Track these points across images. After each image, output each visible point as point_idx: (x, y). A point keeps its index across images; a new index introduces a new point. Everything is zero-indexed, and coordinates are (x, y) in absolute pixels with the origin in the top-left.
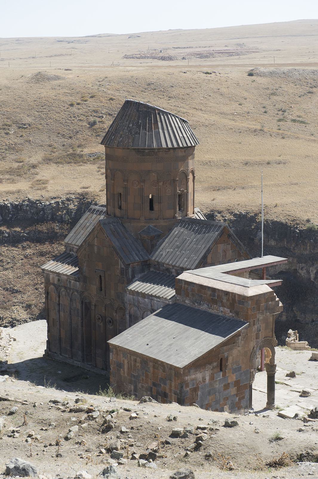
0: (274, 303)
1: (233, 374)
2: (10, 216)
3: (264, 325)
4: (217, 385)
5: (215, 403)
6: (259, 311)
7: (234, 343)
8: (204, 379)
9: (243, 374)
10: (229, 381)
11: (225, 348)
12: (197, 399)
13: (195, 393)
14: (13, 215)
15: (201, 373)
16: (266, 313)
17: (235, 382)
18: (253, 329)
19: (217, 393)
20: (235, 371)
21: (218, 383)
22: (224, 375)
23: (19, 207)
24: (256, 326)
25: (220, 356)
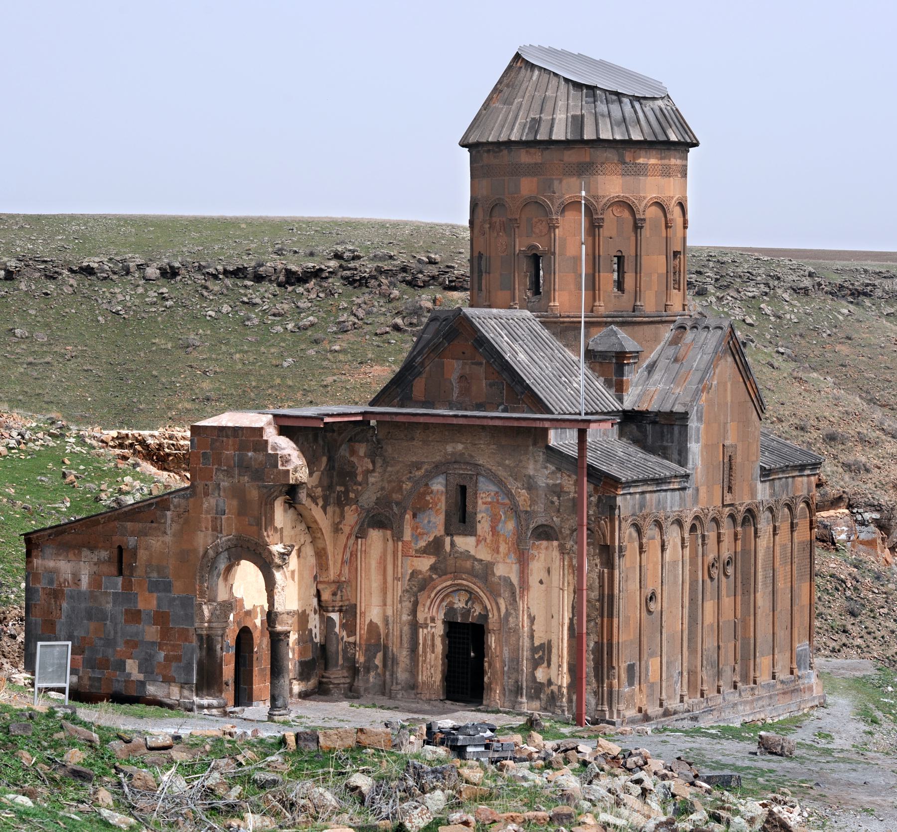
0: (261, 457)
1: (151, 591)
3: (235, 503)
4: (108, 603)
5: (102, 642)
6: (220, 465)
7: (152, 522)
8: (77, 580)
9: (177, 602)
10: (141, 606)
11: (129, 525)
12: (60, 618)
13: (55, 602)
15: (69, 561)
16: (240, 475)
17: (156, 612)
18: (202, 503)
19: (108, 622)
20: (154, 587)
21: (110, 599)
22: (128, 585)
24: (212, 501)
25: (117, 540)
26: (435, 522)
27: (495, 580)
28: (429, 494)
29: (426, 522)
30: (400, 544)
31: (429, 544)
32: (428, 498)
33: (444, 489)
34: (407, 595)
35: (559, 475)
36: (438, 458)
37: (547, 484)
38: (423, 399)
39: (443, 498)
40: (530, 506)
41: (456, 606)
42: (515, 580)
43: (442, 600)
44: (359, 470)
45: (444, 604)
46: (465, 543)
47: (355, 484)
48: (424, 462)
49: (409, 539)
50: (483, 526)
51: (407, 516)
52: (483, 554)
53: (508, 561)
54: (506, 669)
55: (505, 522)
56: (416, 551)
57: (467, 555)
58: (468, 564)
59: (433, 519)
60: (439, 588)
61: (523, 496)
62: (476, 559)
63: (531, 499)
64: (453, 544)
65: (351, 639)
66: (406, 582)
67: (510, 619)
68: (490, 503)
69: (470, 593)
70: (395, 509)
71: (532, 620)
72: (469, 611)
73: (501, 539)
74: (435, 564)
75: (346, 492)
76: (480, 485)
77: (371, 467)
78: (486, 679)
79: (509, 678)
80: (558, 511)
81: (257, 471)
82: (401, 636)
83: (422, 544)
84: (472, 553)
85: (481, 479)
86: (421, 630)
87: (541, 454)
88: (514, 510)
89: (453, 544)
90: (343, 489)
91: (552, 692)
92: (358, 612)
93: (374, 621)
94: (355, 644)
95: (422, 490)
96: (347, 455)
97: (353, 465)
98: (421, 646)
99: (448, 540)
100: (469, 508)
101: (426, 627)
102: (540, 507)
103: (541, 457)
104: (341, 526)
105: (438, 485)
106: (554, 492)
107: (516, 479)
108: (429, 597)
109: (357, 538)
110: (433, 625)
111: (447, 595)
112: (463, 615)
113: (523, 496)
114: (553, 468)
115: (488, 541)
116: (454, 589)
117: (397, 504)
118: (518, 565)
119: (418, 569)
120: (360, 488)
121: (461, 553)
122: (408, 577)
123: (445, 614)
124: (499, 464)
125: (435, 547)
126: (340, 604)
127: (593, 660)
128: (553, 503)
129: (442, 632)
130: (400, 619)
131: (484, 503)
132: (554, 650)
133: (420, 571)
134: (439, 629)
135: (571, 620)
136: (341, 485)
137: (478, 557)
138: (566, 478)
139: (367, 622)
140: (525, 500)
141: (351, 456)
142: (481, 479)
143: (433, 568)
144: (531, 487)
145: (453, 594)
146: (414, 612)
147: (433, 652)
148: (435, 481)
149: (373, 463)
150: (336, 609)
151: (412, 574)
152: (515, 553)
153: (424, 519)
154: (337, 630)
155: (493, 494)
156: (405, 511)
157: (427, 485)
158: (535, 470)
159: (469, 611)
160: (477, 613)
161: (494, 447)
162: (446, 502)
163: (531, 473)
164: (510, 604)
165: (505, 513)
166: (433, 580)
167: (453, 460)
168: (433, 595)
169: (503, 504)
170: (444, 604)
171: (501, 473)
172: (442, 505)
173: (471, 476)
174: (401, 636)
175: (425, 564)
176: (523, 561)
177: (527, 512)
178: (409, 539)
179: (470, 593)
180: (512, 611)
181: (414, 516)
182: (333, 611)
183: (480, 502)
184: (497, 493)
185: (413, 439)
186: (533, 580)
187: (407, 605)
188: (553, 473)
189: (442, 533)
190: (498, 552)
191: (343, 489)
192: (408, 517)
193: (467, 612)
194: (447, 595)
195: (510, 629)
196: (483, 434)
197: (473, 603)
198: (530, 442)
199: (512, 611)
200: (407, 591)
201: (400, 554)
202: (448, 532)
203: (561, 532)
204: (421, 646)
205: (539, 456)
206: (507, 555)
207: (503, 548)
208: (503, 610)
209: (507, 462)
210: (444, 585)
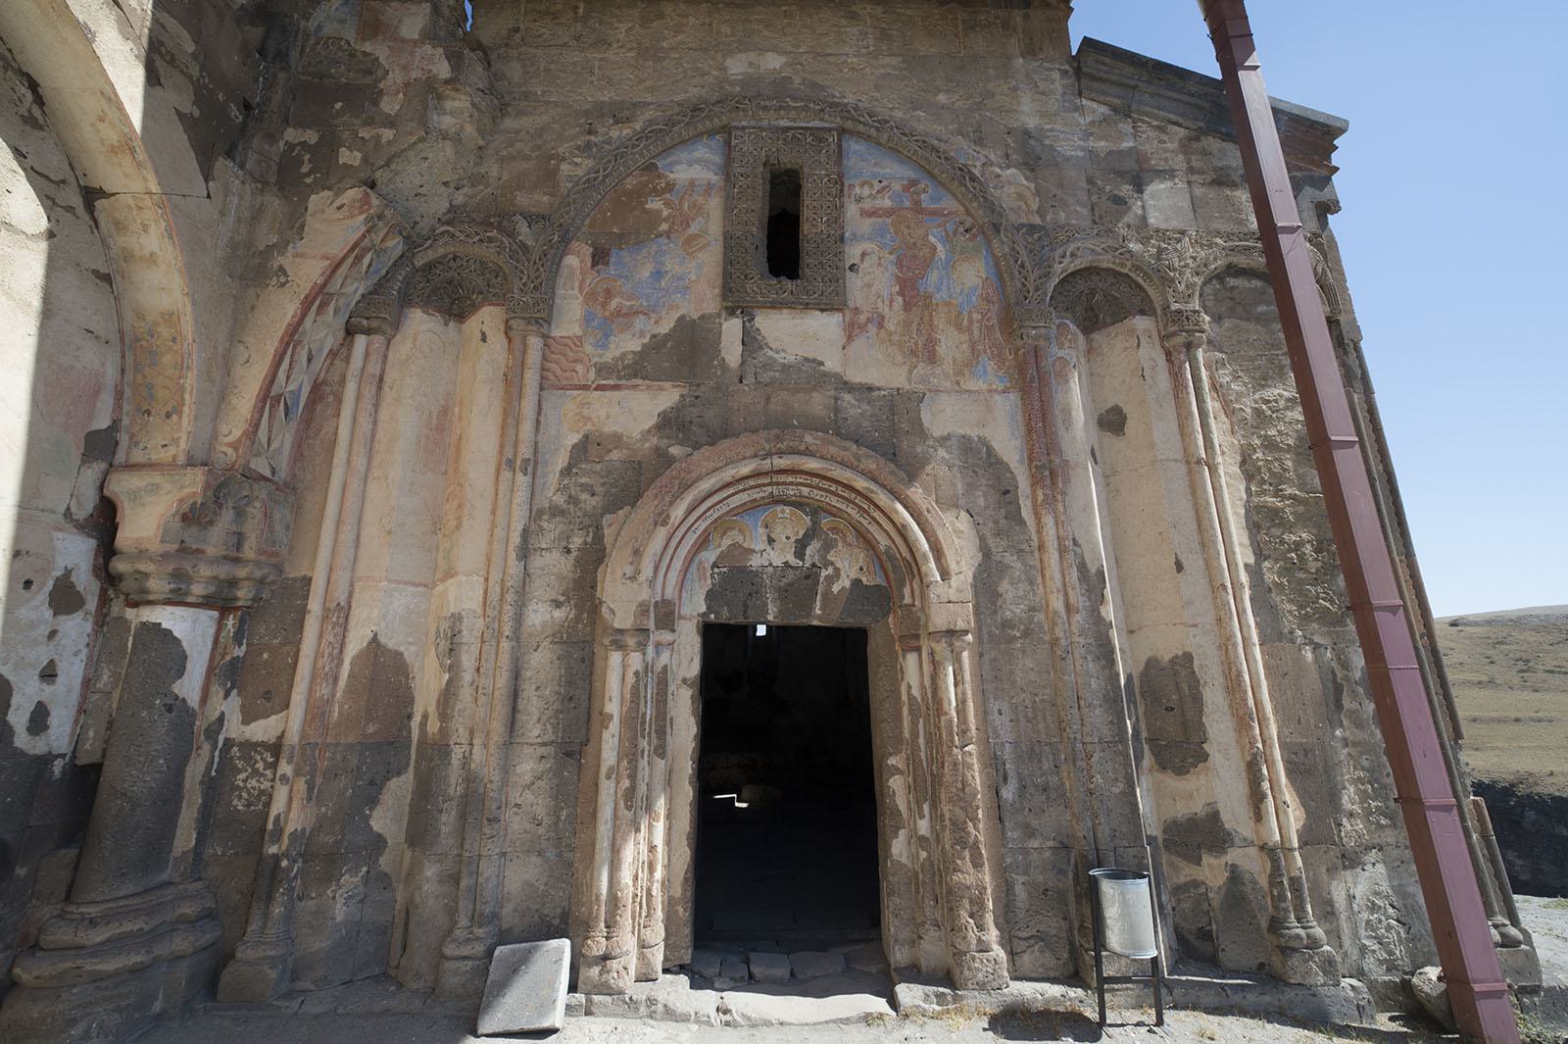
26: (686, 271)
28: (657, 192)
29: (646, 273)
30: (535, 343)
31: (657, 344)
32: (654, 204)
33: (715, 179)
34: (552, 528)
35: (1126, 127)
37: (1092, 153)
39: (715, 205)
40: (1041, 212)
41: (755, 562)
42: (1009, 447)
43: (703, 543)
44: (396, 77)
45: (710, 556)
46: (796, 333)
47: (369, 122)
48: (645, 104)
49: (576, 330)
50: (871, 279)
51: (571, 261)
52: (877, 367)
53: (972, 384)
54: (1008, 793)
55: (950, 265)
56: (601, 369)
57: (812, 376)
58: (817, 403)
59: (672, 265)
60: (706, 485)
61: (1012, 187)
62: (848, 386)
63: (1038, 193)
64: (751, 341)
65: (262, 730)
66: (553, 478)
67: (1004, 586)
68: (889, 213)
69: (815, 511)
70: (524, 231)
71: (1093, 584)
72: (811, 575)
73: (940, 322)
74: (677, 409)
75: (329, 145)
76: (851, 162)
77: (443, 70)
78: (899, 849)
79: (1030, 832)
82: (515, 694)
83: (628, 344)
84: (832, 365)
85: (854, 146)
86: (615, 658)
87: (1056, 75)
88: (987, 224)
89: (751, 341)
90: (311, 136)
91: (1235, 875)
92: (315, 605)
93: (389, 641)
94: (276, 748)
95: (630, 183)
96: (350, 34)
97: (371, 67)
98: (614, 727)
99: (732, 328)
100: (812, 225)
101: (642, 646)
102: (1075, 213)
103: (1057, 83)
104: (285, 260)
105: (694, 168)
107: (980, 142)
108: (662, 519)
109: (350, 332)
110: (666, 636)
111: (721, 526)
112: (784, 593)
113: (1012, 187)
114: (1104, 109)
115: (890, 326)
116: (756, 494)
117: (531, 219)
118: (1014, 397)
119: (609, 428)
120: (388, 134)
121: (786, 368)
122: (561, 460)
123: (710, 596)
124: (915, 106)
125: (685, 352)
126: (223, 571)
129: (694, 669)
130: (519, 619)
131: (865, 213)
132: (1214, 697)
133: (617, 440)
134: (684, 656)
135: (1255, 572)
136: (302, 124)
137: (856, 376)
138: (1152, 134)
139: (355, 644)
140: (1020, 197)
141: (364, 40)
142: (854, 146)
143: (671, 423)
144: (1032, 156)
145: (747, 520)
146: (584, 591)
147: (661, 751)
148: (682, 155)
149: (455, 59)
150: (198, 590)
151: (581, 450)
152: (999, 357)
153: (637, 268)
154: (189, 687)
155: (897, 186)
156: (565, 241)
157: (650, 168)
158: (1043, 115)
159: (811, 575)
160: (845, 582)
161: (895, 61)
162: (728, 209)
163: (1032, 123)
164: (998, 534)
165: (947, 239)
166: (668, 461)
168: (678, 511)
169: (934, 213)
170: (710, 556)
171: (922, 122)
172: (712, 223)
173: (819, 135)
174: (515, 694)
175: (635, 413)
176: (1034, 387)
177: (1032, 228)
178: (576, 330)
179: (815, 511)
180: (1010, 559)
181: (600, 257)
182: (177, 599)
183: (852, 210)
184: (913, 183)
185: (603, 42)
187: (553, 565)
188: (1105, 120)
189: (711, 304)
190: (932, 359)
191: (311, 136)
192: (574, 261)
193: (802, 584)
194: (721, 526)
195: (1006, 624)
196: (855, 31)
197: (828, 546)
198: (1014, 46)
199: (1010, 559)
200: (556, 512)
201: (531, 378)
202: (736, 304)
204: (614, 727)
205: (1053, 81)
207: (950, 344)
209: (942, 98)
210: (728, 474)
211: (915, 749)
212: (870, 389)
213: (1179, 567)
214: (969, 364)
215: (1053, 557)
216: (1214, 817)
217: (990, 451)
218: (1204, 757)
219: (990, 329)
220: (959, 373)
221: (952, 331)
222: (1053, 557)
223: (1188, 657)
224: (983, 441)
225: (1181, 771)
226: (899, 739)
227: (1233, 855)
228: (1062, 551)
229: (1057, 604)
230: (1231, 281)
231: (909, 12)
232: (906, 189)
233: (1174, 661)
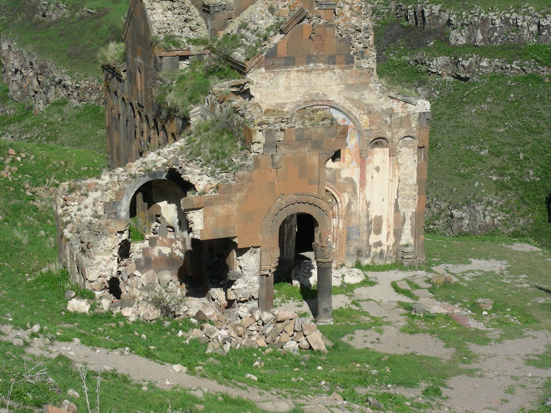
2: (496, 34)
14: (501, 33)
23: (511, 21)
27: (341, 181)
36: (298, 98)
38: (286, 55)
42: (356, 179)
48: (288, 103)
53: (351, 166)
67: (352, 206)
71: (368, 204)
80: (390, 127)
81: (317, 141)
98: (286, 236)
106: (388, 114)
107: (359, 108)
118: (359, 168)
127: (411, 224)
128: (386, 122)
140: (366, 123)
152: (357, 160)
161: (343, 86)
164: (352, 196)
167: (310, 99)
177: (367, 130)
180: (354, 201)
184: (344, 119)
186: (368, 177)
195: (352, 213)
199: (354, 201)
203: (392, 142)
204: (286, 236)
206: (350, 162)
208: (347, 201)
211: (333, 234)
212: (331, 169)
213: (383, 200)
214: (351, 162)
215: (361, 201)
216: (380, 242)
217: (352, 180)
218: (381, 232)
219: (356, 154)
220: (349, 164)
221: (348, 154)
222: (361, 201)
223: (382, 216)
224: (351, 178)
225: (377, 234)
226: (330, 232)
227: (382, 247)
228: (363, 200)
229: (361, 209)
230: (405, 139)
231: (348, 71)
232: (342, 121)
233: (379, 216)
